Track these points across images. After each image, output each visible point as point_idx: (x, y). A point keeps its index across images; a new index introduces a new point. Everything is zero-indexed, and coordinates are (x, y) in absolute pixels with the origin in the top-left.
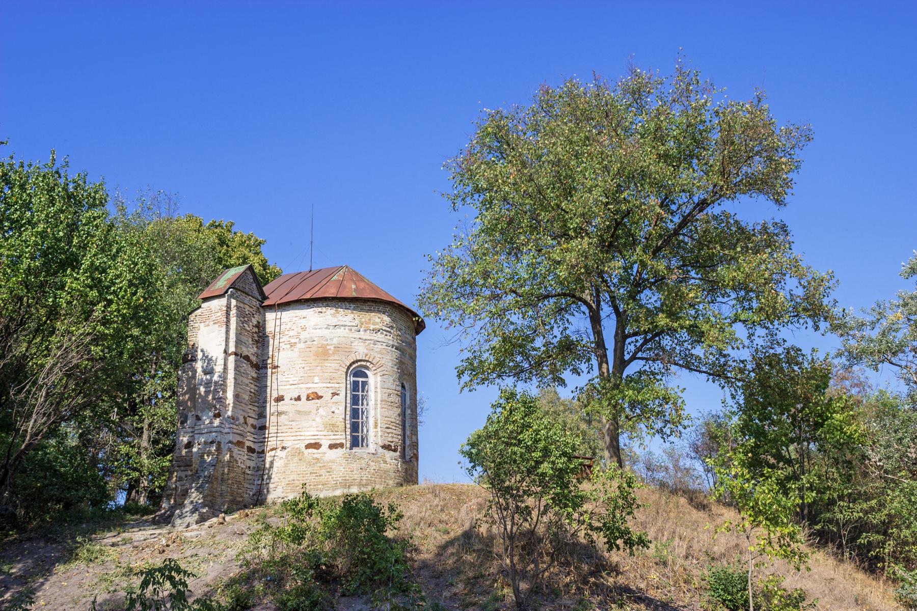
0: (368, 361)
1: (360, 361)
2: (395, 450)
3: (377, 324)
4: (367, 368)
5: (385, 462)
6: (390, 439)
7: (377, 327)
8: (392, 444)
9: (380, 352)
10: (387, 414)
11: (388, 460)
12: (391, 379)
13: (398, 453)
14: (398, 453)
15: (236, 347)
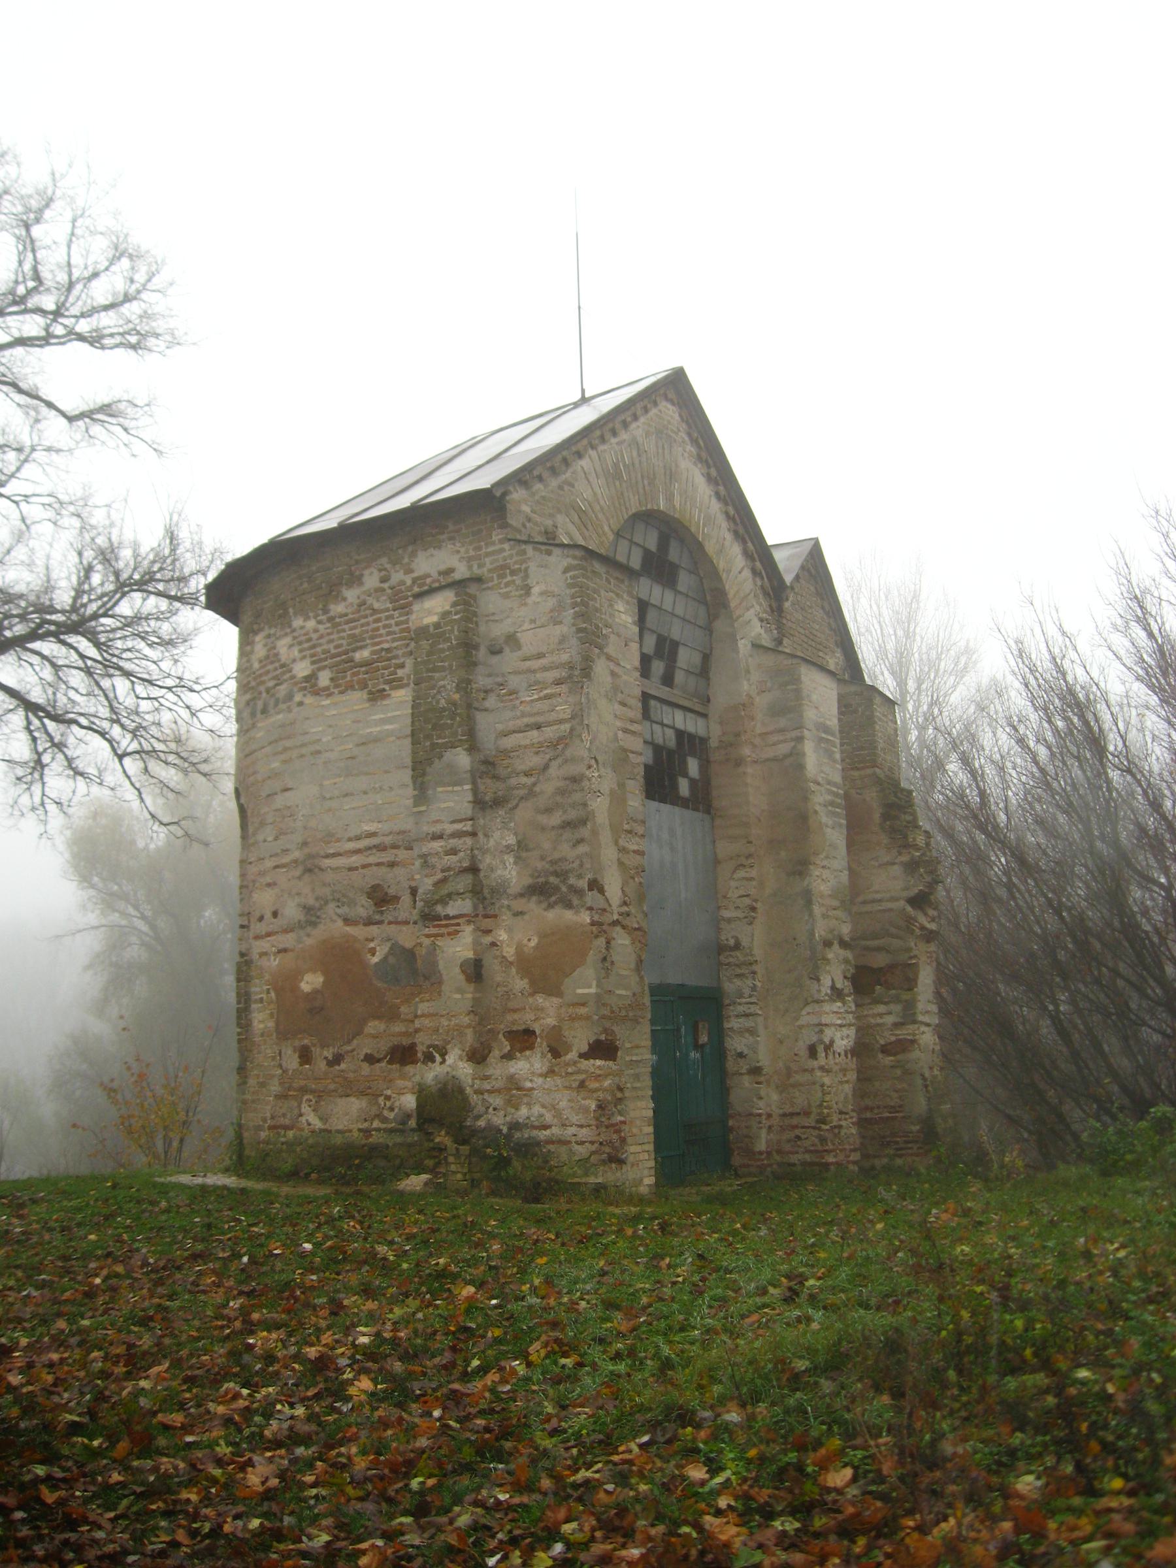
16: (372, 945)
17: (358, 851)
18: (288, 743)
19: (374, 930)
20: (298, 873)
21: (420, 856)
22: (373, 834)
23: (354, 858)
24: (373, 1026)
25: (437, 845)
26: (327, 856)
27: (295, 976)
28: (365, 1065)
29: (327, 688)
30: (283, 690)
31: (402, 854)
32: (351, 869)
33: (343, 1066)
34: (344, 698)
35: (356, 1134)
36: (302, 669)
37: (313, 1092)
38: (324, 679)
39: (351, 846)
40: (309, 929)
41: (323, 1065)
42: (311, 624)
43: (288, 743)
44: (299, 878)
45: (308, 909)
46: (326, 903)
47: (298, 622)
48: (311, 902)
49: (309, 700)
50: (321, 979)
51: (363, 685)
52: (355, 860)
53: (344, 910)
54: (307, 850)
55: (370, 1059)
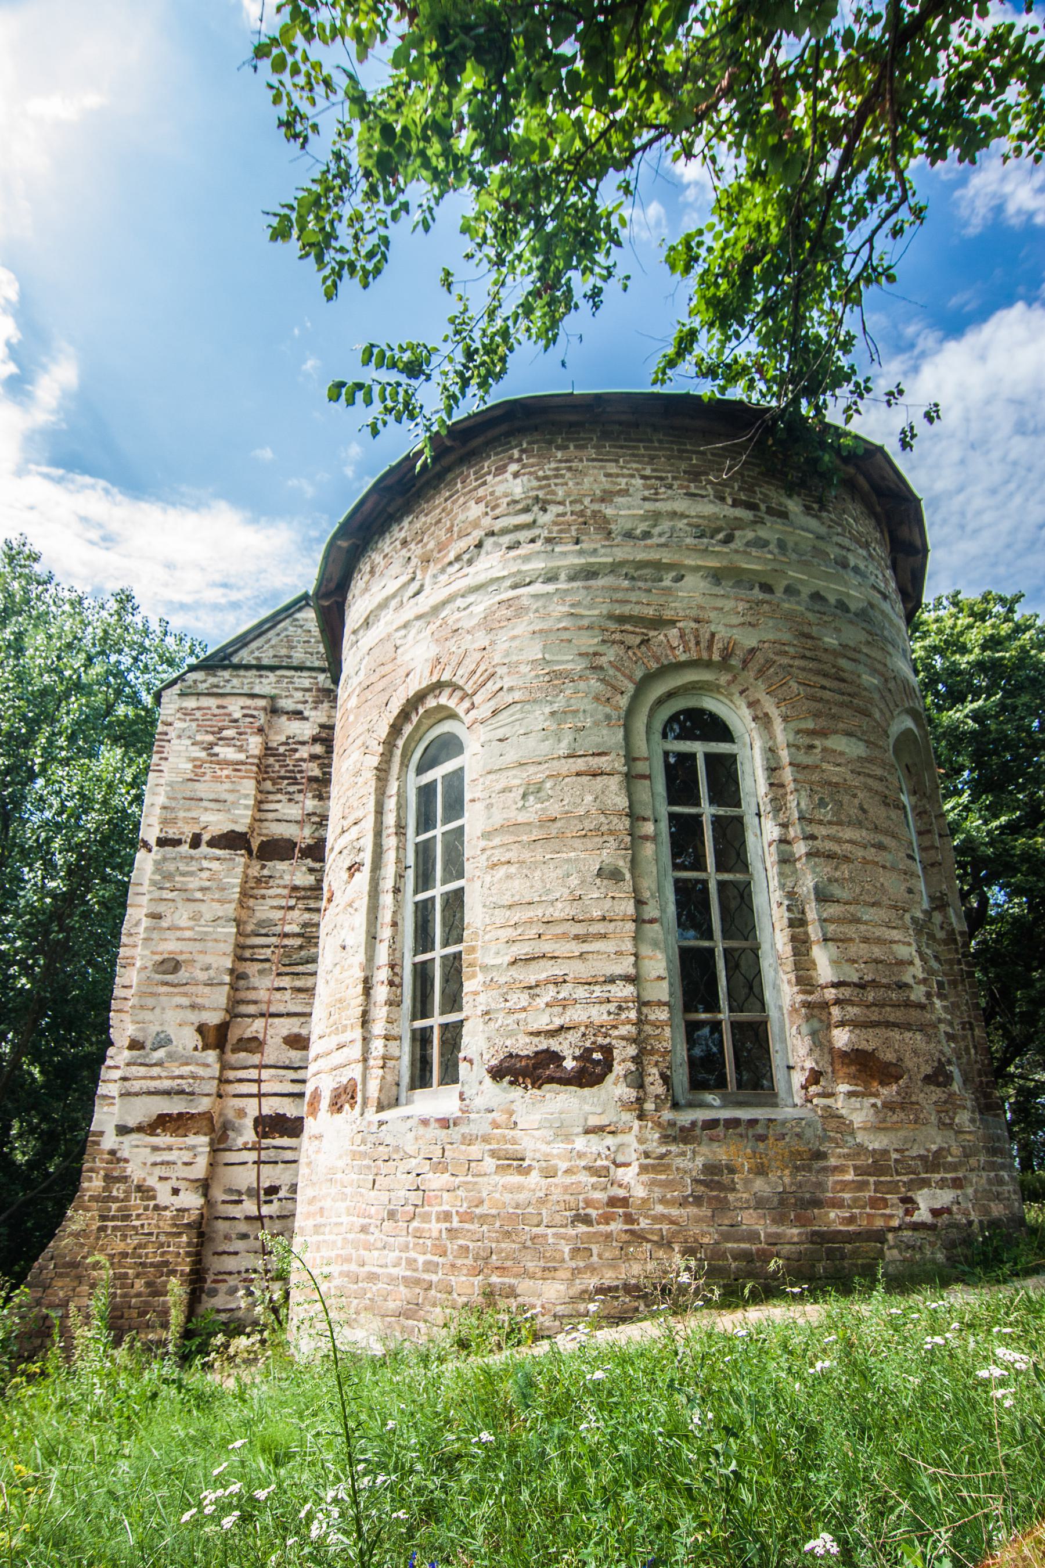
0: (439, 686)
1: (420, 697)
2: (590, 1073)
3: (476, 524)
4: (453, 716)
5: (514, 1162)
6: (543, 1021)
7: (477, 534)
8: (568, 1048)
9: (488, 624)
10: (519, 888)
11: (533, 1143)
12: (539, 717)
13: (616, 1088)
14: (616, 1088)
15: (164, 822)
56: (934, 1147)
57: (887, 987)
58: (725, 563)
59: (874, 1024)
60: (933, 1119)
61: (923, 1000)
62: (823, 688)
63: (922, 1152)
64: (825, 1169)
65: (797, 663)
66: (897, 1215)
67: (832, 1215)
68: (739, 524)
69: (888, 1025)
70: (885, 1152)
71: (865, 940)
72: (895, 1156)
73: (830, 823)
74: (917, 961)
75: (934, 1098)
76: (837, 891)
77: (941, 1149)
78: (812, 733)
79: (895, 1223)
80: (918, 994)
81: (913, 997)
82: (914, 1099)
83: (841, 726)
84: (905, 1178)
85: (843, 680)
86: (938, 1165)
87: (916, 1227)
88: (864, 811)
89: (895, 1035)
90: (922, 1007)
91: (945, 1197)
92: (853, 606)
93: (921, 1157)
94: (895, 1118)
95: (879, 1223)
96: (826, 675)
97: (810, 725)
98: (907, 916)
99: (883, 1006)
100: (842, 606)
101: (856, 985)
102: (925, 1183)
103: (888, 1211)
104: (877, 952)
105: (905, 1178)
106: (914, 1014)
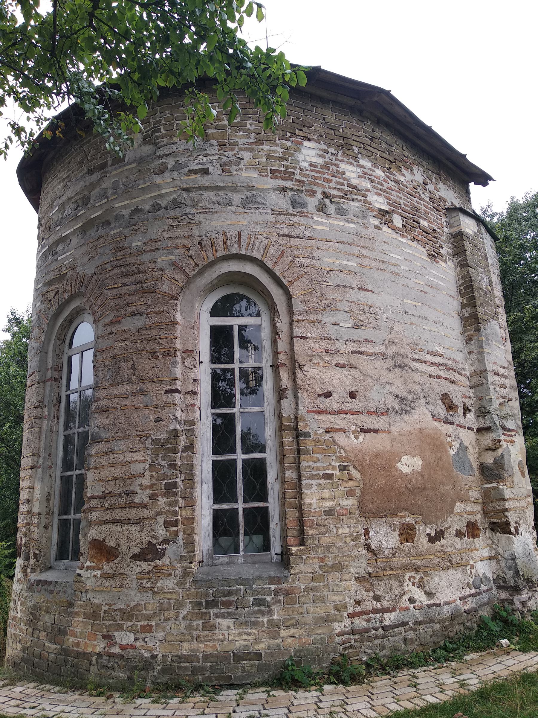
16: (449, 440)
17: (434, 364)
18: (364, 252)
19: (450, 429)
20: (389, 363)
21: (493, 384)
22: (441, 356)
23: (432, 368)
24: (459, 507)
25: (497, 378)
26: (414, 360)
27: (395, 457)
28: (457, 539)
29: (399, 229)
30: (354, 206)
31: (457, 377)
32: (431, 376)
33: (443, 541)
34: (410, 243)
35: (459, 602)
36: (379, 202)
37: (416, 569)
38: (398, 222)
39: (429, 358)
40: (405, 417)
41: (424, 541)
42: (379, 172)
43: (364, 252)
44: (389, 369)
45: (402, 400)
46: (418, 398)
47: (366, 163)
48: (404, 394)
49: (385, 228)
50: (420, 463)
51: (424, 245)
52: (433, 370)
53: (430, 407)
54: (395, 349)
55: (459, 534)
56: (133, 604)
57: (119, 495)
58: (85, 221)
59: (105, 523)
60: (135, 584)
61: (147, 500)
62: (124, 285)
63: (123, 607)
64: (71, 613)
65: (115, 272)
66: (100, 646)
67: (70, 640)
68: (93, 186)
69: (115, 522)
70: (100, 605)
71: (112, 465)
72: (105, 608)
73: (111, 386)
74: (148, 474)
75: (138, 570)
76: (103, 435)
77: (138, 605)
78: (111, 323)
79: (98, 650)
80: (142, 496)
81: (136, 500)
82: (122, 571)
83: (130, 309)
84: (107, 623)
85: (140, 272)
86: (132, 616)
87: (111, 656)
88: (134, 369)
89: (116, 529)
90: (144, 506)
91: (130, 638)
92: (163, 203)
93: (120, 610)
94: (107, 584)
95: (90, 650)
96: (126, 275)
97: (111, 318)
98: (149, 440)
99: (114, 509)
100: (156, 207)
101: (99, 497)
102: (120, 628)
103: (95, 643)
104: (119, 472)
105: (107, 623)
106: (136, 513)
